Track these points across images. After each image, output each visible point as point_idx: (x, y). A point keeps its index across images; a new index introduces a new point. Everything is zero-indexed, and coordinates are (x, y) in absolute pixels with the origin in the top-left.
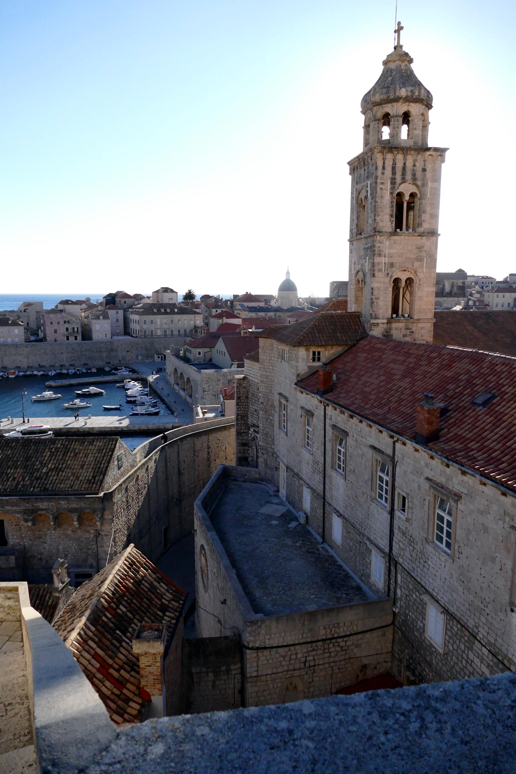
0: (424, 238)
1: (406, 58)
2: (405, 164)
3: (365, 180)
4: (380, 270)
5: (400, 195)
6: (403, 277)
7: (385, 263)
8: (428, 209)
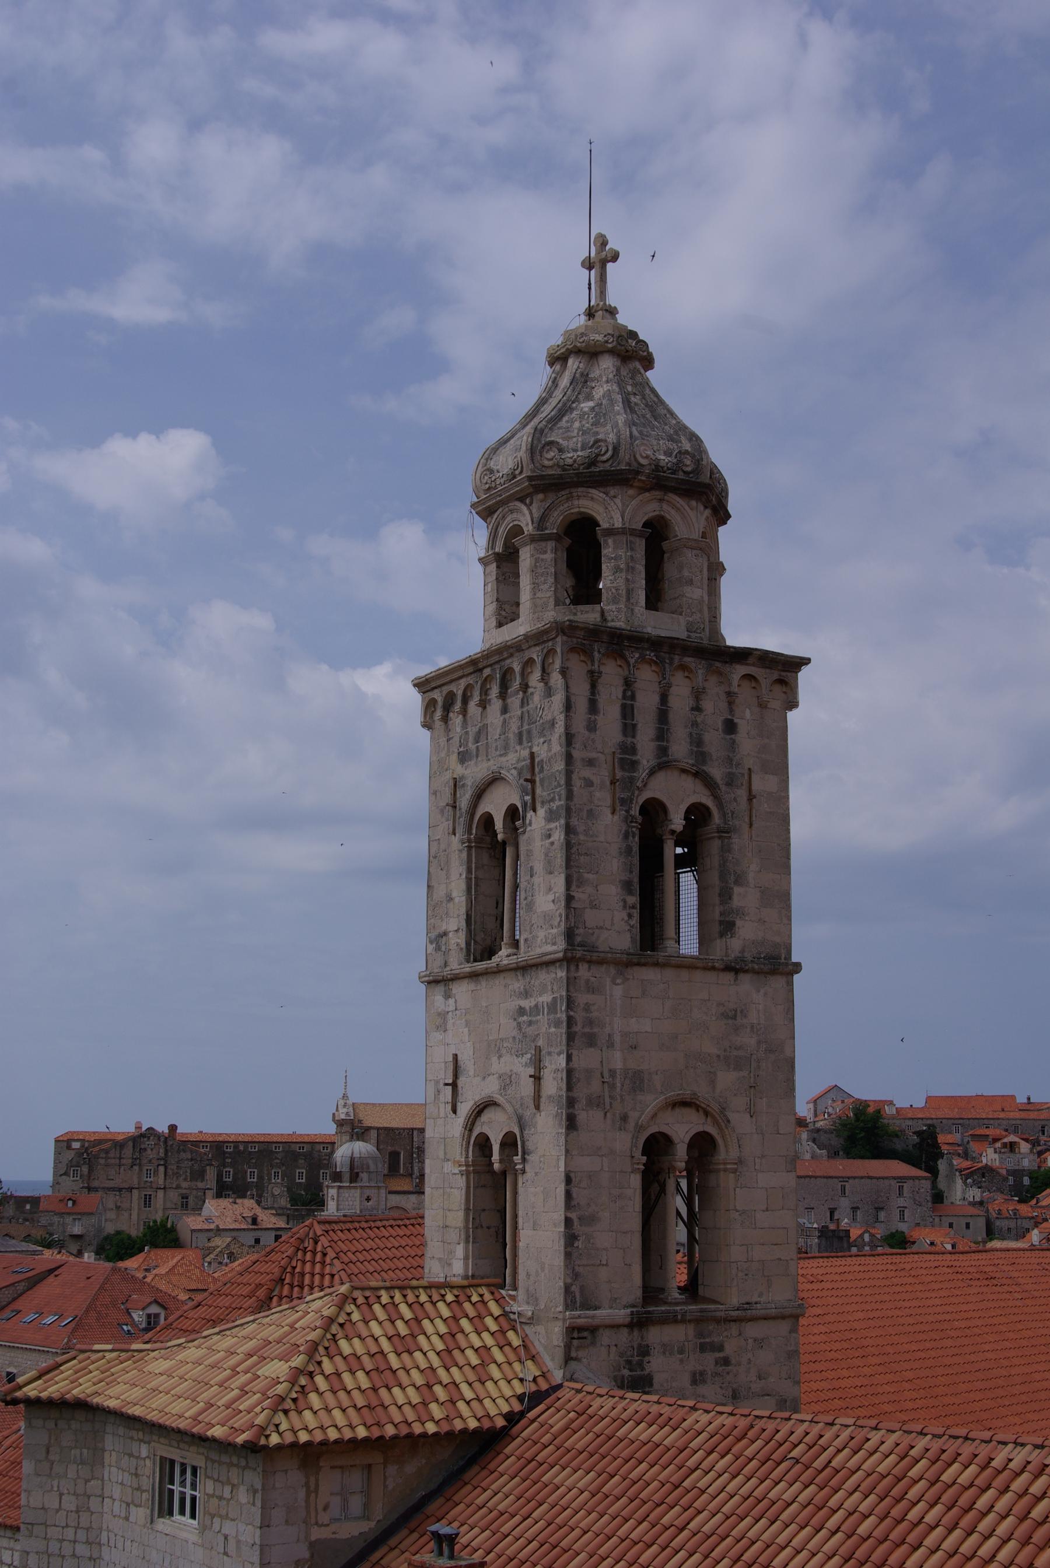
0: (745, 978)
1: (632, 353)
2: (664, 698)
3: (506, 747)
5: (653, 812)
6: (682, 1129)
8: (752, 869)
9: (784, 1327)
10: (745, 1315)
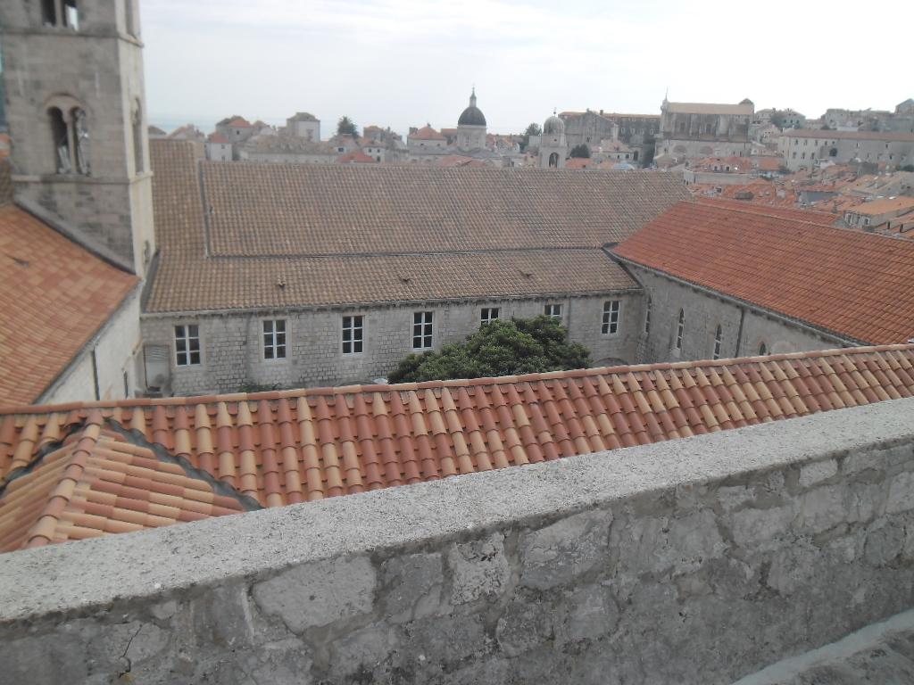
4: (17, 93)
6: (65, 106)
7: (25, 82)
9: (120, 189)
10: (98, 182)
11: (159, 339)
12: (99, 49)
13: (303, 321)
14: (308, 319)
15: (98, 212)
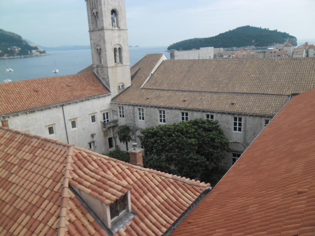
5: (94, 13)
6: (98, 48)
9: (106, 69)
11: (115, 109)
12: (101, 32)
13: (148, 110)
14: (149, 109)
15: (104, 75)
